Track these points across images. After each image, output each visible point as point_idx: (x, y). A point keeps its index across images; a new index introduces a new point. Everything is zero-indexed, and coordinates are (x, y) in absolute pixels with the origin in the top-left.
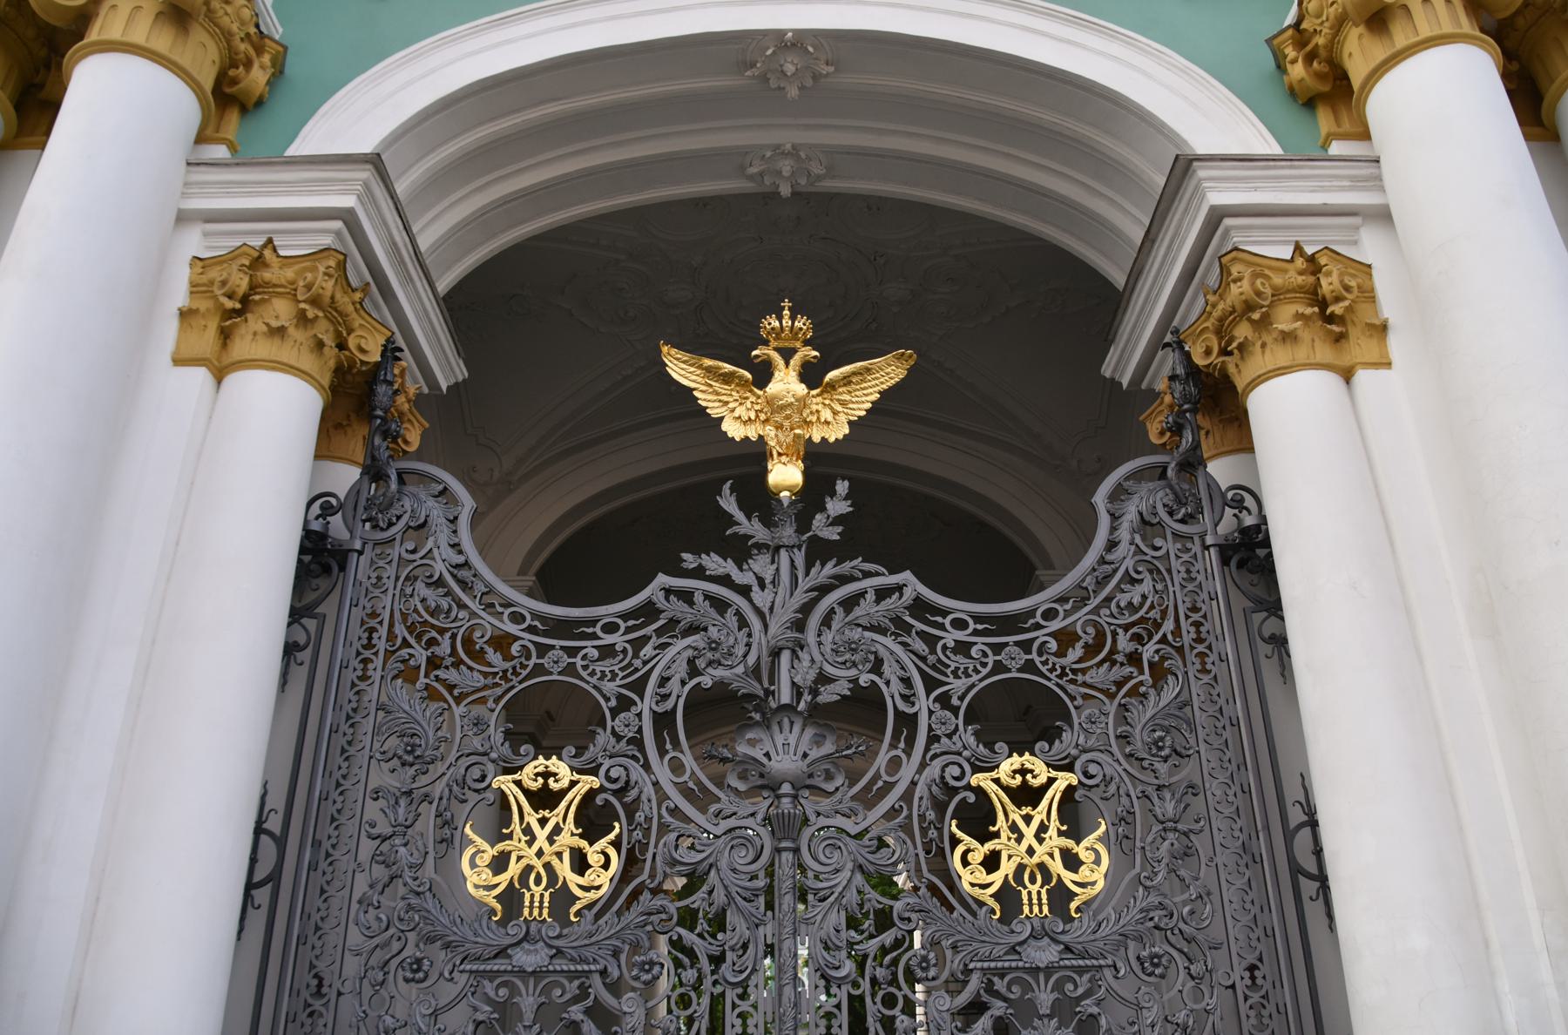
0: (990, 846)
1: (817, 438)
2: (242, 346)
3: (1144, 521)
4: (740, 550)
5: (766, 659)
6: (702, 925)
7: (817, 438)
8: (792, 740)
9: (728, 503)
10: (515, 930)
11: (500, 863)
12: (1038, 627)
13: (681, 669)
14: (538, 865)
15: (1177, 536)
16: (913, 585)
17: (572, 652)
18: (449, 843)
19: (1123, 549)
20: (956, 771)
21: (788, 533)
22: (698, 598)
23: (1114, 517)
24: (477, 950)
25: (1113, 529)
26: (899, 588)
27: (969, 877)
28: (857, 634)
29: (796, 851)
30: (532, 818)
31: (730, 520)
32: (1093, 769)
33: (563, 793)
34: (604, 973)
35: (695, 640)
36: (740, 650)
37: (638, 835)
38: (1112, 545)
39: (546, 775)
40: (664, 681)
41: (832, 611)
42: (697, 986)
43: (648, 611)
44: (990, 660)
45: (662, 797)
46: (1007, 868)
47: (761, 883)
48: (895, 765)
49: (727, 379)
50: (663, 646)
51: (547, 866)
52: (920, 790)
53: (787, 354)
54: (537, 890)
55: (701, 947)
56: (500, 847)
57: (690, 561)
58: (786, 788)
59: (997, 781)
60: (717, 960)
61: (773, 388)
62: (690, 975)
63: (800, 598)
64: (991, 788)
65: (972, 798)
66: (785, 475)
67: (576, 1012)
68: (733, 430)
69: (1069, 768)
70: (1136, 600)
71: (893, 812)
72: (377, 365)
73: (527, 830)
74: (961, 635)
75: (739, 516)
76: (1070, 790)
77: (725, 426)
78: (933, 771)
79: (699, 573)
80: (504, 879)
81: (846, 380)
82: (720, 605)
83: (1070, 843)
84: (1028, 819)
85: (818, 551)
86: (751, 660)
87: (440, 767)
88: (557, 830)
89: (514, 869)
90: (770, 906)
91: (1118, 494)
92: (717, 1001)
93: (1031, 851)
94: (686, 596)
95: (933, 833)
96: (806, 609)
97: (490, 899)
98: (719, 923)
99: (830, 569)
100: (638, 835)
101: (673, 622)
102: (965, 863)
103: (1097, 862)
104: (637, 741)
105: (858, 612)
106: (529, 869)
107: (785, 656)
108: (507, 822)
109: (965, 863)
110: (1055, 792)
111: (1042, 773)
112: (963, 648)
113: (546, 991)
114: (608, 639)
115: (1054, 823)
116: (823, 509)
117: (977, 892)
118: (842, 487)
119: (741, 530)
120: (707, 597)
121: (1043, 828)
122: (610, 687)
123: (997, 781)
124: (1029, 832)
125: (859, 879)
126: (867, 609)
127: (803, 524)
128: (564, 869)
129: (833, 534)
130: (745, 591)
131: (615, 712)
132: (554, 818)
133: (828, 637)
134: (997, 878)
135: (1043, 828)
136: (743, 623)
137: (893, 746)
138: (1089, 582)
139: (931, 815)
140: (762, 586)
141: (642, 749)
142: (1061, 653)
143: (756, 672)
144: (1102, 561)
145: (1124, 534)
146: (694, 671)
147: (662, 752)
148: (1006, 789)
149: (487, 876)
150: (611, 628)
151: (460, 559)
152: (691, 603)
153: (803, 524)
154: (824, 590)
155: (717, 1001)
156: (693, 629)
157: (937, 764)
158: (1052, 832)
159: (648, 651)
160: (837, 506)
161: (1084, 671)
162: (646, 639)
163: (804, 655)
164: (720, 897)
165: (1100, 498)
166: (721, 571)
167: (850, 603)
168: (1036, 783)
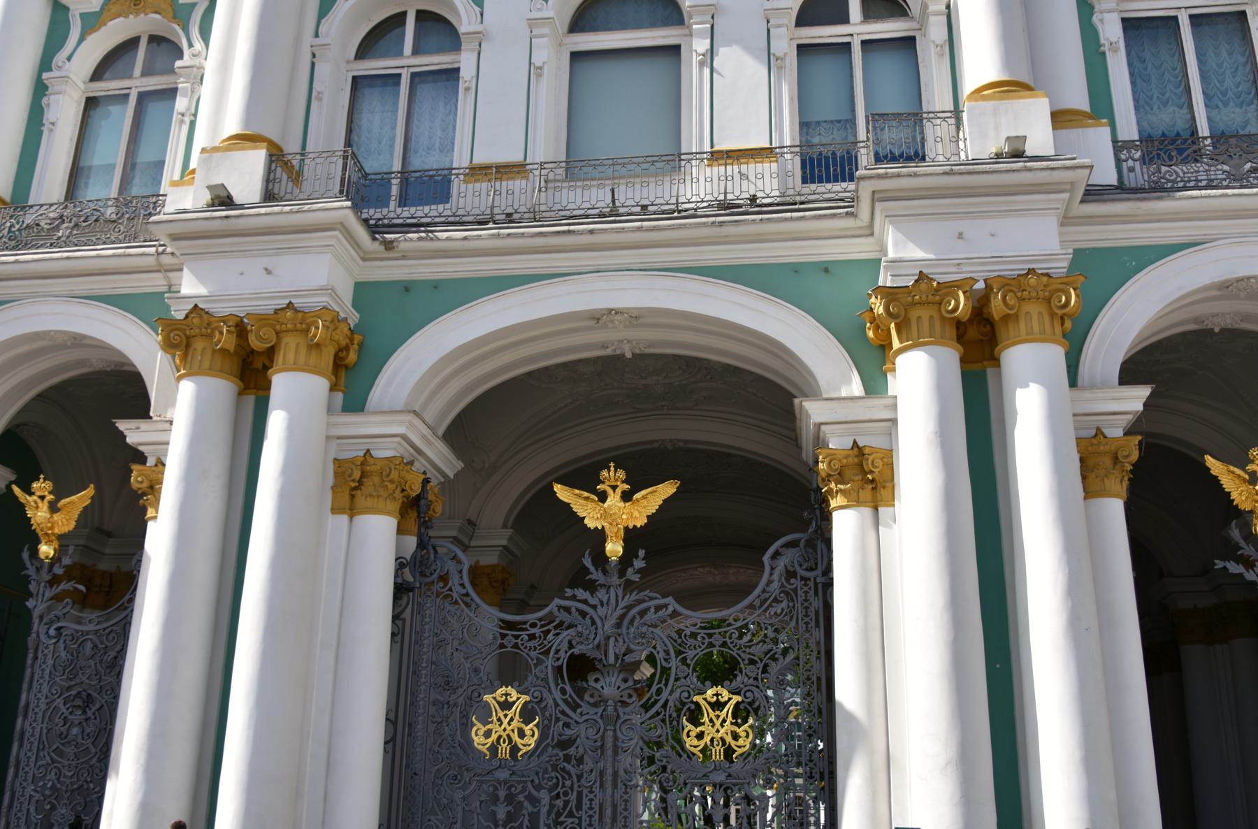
0: (699, 729)
1: (631, 527)
2: (360, 501)
3: (787, 571)
4: (591, 587)
5: (603, 642)
6: (574, 762)
7: (631, 527)
8: (613, 680)
9: (587, 562)
10: (495, 763)
11: (488, 734)
12: (729, 625)
13: (565, 646)
14: (504, 735)
15: (803, 578)
16: (673, 604)
17: (517, 637)
18: (467, 726)
19: (775, 585)
20: (686, 695)
21: (615, 580)
22: (573, 610)
23: (772, 569)
24: (479, 771)
25: (771, 574)
26: (666, 606)
27: (690, 742)
28: (644, 629)
29: (615, 731)
30: (501, 714)
31: (588, 572)
32: (748, 694)
33: (514, 703)
34: (532, 781)
35: (572, 631)
36: (592, 636)
37: (546, 722)
38: (769, 583)
39: (507, 695)
40: (557, 651)
41: (634, 617)
42: (572, 788)
43: (550, 618)
44: (707, 641)
45: (557, 705)
46: (707, 739)
47: (599, 744)
48: (659, 692)
49: (587, 499)
50: (557, 634)
51: (508, 736)
52: (671, 703)
53: (614, 488)
54: (504, 746)
55: (573, 771)
56: (489, 726)
57: (569, 592)
58: (610, 702)
59: (705, 699)
60: (579, 777)
61: (609, 502)
62: (568, 783)
63: (619, 612)
64: (702, 703)
65: (693, 707)
66: (614, 548)
67: (521, 798)
68: (590, 523)
69: (738, 693)
70: (779, 611)
71: (658, 713)
72: (418, 496)
73: (499, 720)
74: (694, 629)
75: (592, 569)
76: (738, 704)
77: (586, 521)
78: (676, 694)
79: (574, 598)
80: (490, 740)
81: (644, 497)
82: (583, 614)
83: (736, 728)
84: (718, 717)
85: (628, 586)
86: (596, 642)
87: (460, 691)
88: (512, 719)
89: (494, 737)
90: (602, 754)
91: (776, 555)
92: (580, 794)
93: (718, 731)
94: (567, 609)
95: (675, 723)
96: (622, 617)
97: (484, 749)
98: (580, 761)
99: (634, 596)
100: (546, 722)
101: (561, 623)
102: (688, 736)
103: (747, 736)
104: (545, 680)
105: (646, 617)
106: (500, 737)
107: (612, 640)
108: (491, 716)
109: (688, 736)
110: (730, 707)
111: (725, 695)
112: (694, 635)
113: (509, 788)
114: (533, 631)
115: (730, 719)
116: (632, 565)
117: (692, 749)
118: (642, 553)
119: (593, 577)
120: (577, 610)
121: (724, 721)
122: (533, 654)
123: (705, 699)
124: (718, 723)
125: (641, 743)
126: (651, 616)
127: (622, 573)
128: (515, 737)
129: (636, 578)
130: (594, 607)
131: (536, 666)
132: (510, 713)
133: (632, 630)
134: (702, 743)
135: (724, 721)
136: (593, 623)
137: (659, 682)
138: (757, 603)
139: (675, 715)
140: (602, 605)
141: (548, 683)
142: (740, 638)
143: (598, 646)
144: (764, 591)
145: (775, 577)
146: (571, 646)
147: (557, 685)
148: (709, 703)
149: (482, 740)
150: (533, 625)
151: (464, 591)
152: (570, 613)
153: (622, 573)
154: (629, 608)
155: (580, 794)
156: (570, 626)
157: (679, 691)
158: (728, 722)
159: (550, 636)
160: (639, 563)
161: (750, 647)
162: (549, 631)
163: (621, 640)
164: (581, 750)
165: (766, 558)
166: (583, 598)
167: (643, 613)
168: (722, 700)
